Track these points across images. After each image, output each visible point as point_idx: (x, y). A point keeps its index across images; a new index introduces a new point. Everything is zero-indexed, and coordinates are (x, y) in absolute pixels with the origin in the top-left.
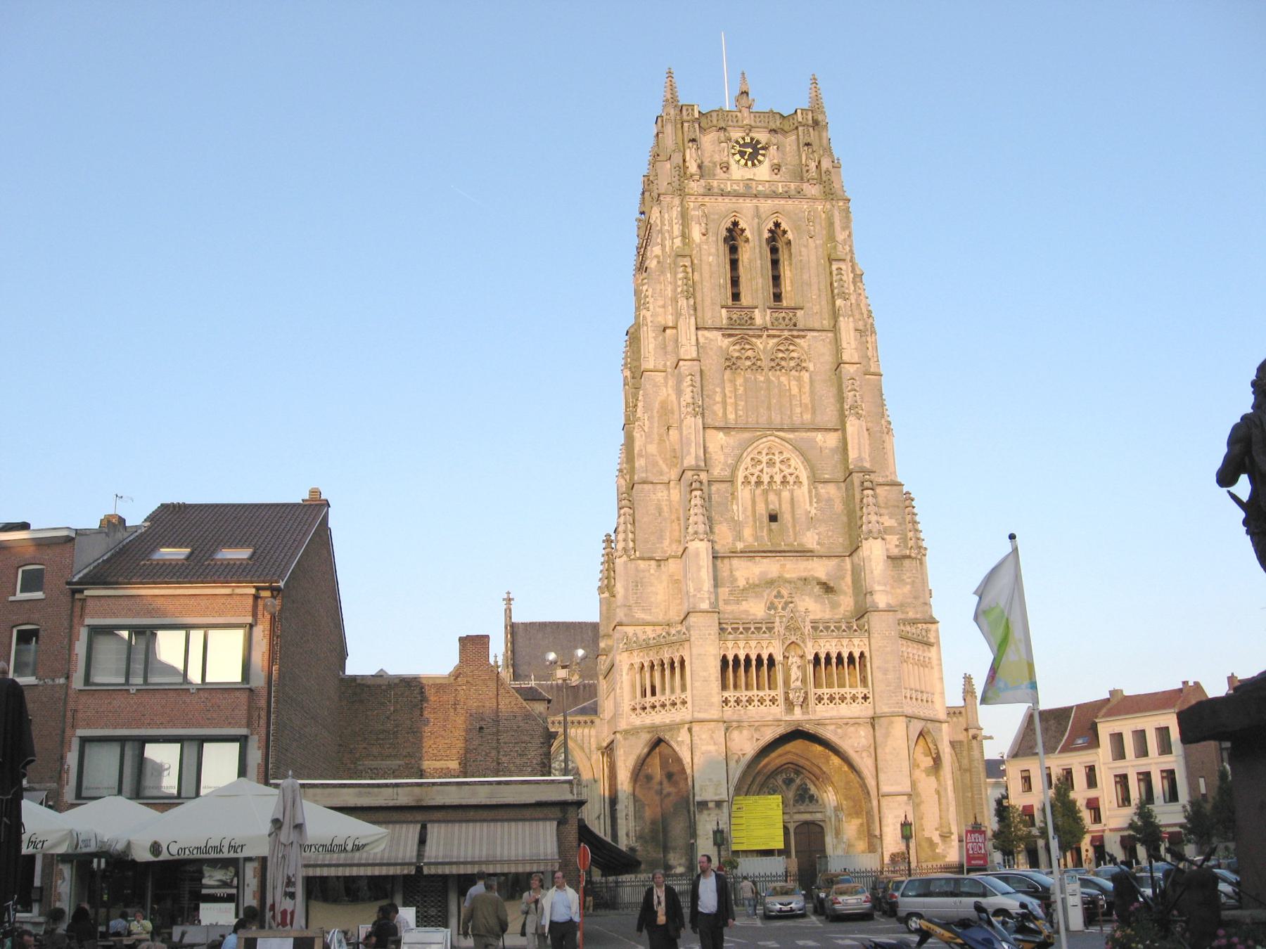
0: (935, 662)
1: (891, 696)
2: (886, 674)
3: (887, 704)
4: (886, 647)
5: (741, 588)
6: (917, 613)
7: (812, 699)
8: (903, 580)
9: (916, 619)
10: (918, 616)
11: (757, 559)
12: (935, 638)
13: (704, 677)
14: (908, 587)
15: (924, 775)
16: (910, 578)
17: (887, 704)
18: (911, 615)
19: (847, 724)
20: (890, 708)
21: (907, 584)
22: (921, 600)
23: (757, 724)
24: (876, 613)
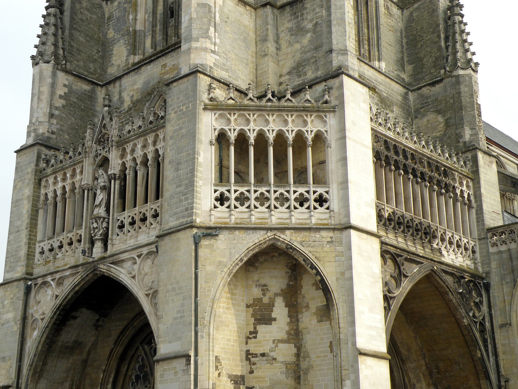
0: (332, 138)
1: (181, 201)
2: (177, 170)
3: (175, 214)
4: (181, 128)
5: (126, 109)
6: (317, 69)
7: (113, 229)
8: (302, 29)
9: (317, 78)
10: (319, 73)
11: (143, 68)
12: (337, 98)
13: (18, 226)
14: (309, 35)
15: (314, 321)
16: (311, 21)
17: (175, 214)
18: (310, 75)
19: (139, 256)
20: (177, 219)
21: (307, 32)
22: (325, 48)
23: (58, 276)
24: (175, 84)
